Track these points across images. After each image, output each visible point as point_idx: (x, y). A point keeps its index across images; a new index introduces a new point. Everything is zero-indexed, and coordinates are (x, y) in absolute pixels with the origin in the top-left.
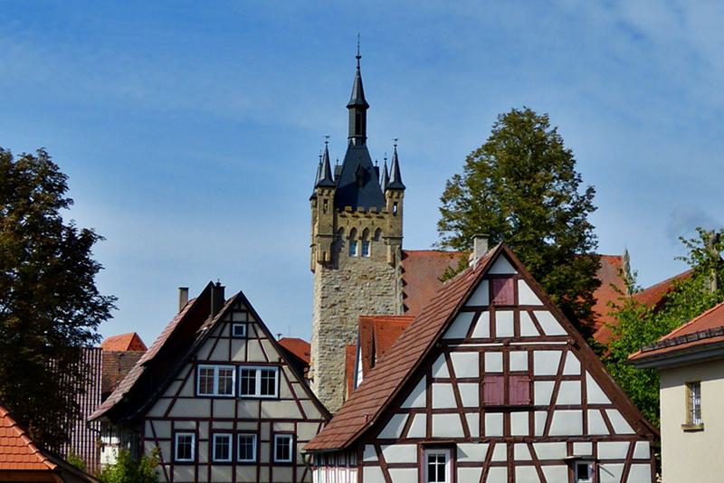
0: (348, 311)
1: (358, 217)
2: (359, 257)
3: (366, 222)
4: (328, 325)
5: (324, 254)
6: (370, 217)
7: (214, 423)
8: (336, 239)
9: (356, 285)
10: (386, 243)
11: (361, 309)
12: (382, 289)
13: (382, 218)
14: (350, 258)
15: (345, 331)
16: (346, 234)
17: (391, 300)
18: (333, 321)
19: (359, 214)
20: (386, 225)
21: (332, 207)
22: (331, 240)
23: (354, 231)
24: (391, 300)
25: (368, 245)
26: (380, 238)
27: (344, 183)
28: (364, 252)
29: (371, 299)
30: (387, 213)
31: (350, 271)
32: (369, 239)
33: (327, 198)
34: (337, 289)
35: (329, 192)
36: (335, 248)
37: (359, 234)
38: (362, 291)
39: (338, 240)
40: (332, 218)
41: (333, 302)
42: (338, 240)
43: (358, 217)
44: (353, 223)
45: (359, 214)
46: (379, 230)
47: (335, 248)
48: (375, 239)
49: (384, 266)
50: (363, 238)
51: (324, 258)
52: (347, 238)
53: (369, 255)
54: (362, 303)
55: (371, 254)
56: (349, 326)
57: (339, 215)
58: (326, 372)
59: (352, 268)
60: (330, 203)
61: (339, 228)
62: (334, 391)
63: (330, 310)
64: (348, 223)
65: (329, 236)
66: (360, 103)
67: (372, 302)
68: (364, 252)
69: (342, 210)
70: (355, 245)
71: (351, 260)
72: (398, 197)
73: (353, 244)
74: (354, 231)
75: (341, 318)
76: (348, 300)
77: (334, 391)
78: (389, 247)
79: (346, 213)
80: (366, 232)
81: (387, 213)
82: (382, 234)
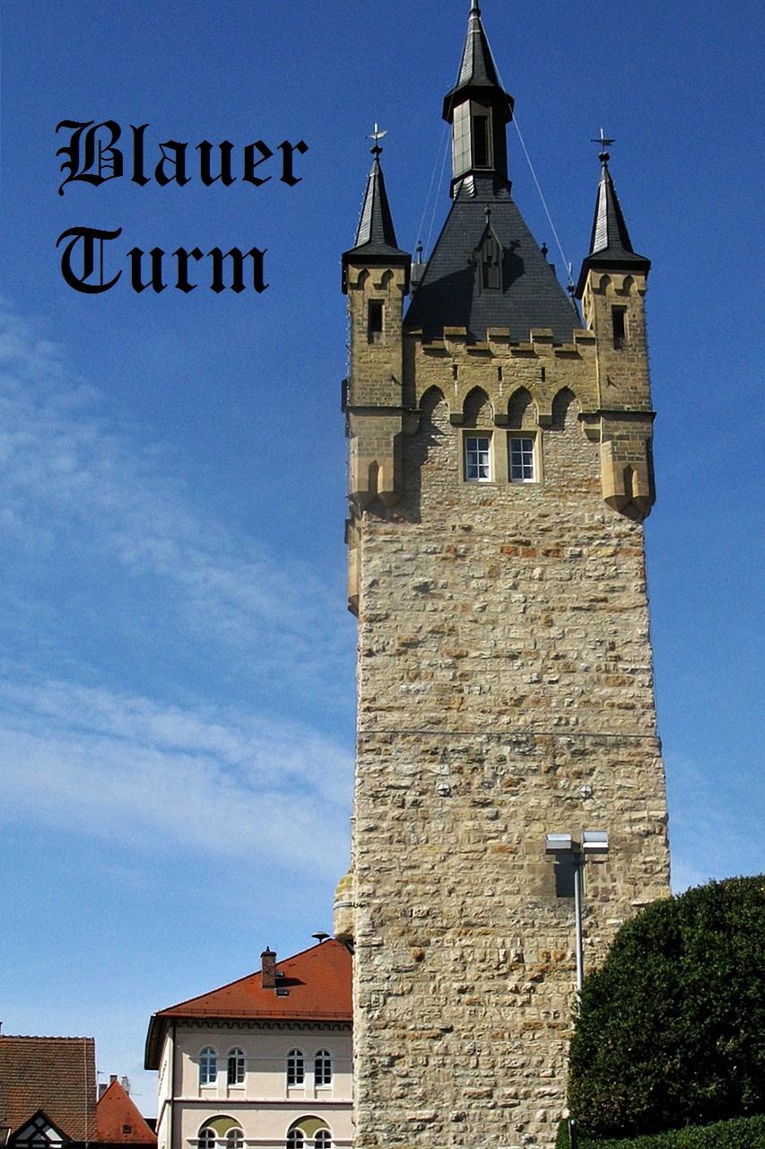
0: (466, 666)
1: (488, 354)
2: (499, 484)
3: (520, 371)
4: (392, 718)
5: (373, 469)
6: (530, 354)
7: (34, 1130)
8: (412, 429)
9: (494, 574)
10: (593, 437)
11: (513, 657)
12: (588, 588)
13: (574, 355)
14: (463, 488)
15: (456, 734)
16: (451, 404)
17: (627, 625)
18: (411, 701)
19: (493, 346)
20: (595, 376)
21: (397, 324)
22: (395, 424)
23: (476, 398)
24: (627, 625)
25: (529, 446)
26: (570, 421)
27: (430, 280)
28: (518, 467)
29: (549, 623)
30: (590, 341)
31: (468, 529)
32: (529, 423)
33: (376, 295)
34: (423, 588)
35: (387, 277)
36: (411, 450)
37: (496, 404)
38: (518, 596)
39: (420, 429)
40: (397, 356)
41: (408, 633)
42: (420, 429)
43: (488, 354)
44: (474, 374)
45: (493, 346)
46: (565, 396)
47: (411, 450)
48: (554, 422)
49: (592, 511)
50: (511, 419)
51: (373, 483)
52: (456, 422)
53: (536, 478)
54: (517, 636)
55: (544, 473)
56: (472, 718)
57: (420, 349)
58: (388, 888)
59: (477, 520)
60: (391, 315)
61: (421, 391)
62: (420, 958)
63: (400, 663)
64: (450, 374)
65: (391, 411)
66: (483, 81)
67: (554, 632)
68: (518, 467)
69: (432, 333)
70: (485, 446)
71: (472, 493)
72: (624, 292)
73: (475, 444)
74: (476, 398)
75: (443, 690)
76: (464, 627)
77: (420, 958)
78: (605, 448)
79: (446, 343)
80: (520, 400)
81: (590, 341)
82: (576, 407)
